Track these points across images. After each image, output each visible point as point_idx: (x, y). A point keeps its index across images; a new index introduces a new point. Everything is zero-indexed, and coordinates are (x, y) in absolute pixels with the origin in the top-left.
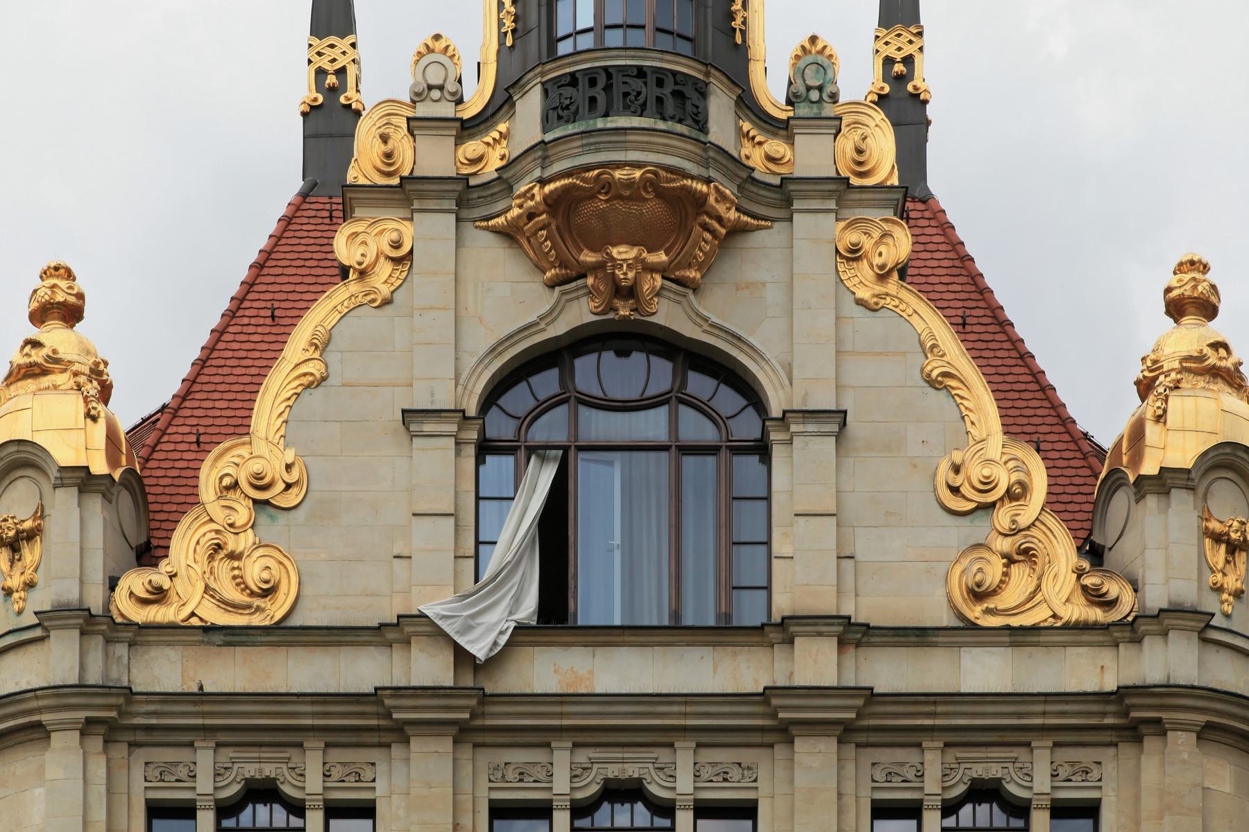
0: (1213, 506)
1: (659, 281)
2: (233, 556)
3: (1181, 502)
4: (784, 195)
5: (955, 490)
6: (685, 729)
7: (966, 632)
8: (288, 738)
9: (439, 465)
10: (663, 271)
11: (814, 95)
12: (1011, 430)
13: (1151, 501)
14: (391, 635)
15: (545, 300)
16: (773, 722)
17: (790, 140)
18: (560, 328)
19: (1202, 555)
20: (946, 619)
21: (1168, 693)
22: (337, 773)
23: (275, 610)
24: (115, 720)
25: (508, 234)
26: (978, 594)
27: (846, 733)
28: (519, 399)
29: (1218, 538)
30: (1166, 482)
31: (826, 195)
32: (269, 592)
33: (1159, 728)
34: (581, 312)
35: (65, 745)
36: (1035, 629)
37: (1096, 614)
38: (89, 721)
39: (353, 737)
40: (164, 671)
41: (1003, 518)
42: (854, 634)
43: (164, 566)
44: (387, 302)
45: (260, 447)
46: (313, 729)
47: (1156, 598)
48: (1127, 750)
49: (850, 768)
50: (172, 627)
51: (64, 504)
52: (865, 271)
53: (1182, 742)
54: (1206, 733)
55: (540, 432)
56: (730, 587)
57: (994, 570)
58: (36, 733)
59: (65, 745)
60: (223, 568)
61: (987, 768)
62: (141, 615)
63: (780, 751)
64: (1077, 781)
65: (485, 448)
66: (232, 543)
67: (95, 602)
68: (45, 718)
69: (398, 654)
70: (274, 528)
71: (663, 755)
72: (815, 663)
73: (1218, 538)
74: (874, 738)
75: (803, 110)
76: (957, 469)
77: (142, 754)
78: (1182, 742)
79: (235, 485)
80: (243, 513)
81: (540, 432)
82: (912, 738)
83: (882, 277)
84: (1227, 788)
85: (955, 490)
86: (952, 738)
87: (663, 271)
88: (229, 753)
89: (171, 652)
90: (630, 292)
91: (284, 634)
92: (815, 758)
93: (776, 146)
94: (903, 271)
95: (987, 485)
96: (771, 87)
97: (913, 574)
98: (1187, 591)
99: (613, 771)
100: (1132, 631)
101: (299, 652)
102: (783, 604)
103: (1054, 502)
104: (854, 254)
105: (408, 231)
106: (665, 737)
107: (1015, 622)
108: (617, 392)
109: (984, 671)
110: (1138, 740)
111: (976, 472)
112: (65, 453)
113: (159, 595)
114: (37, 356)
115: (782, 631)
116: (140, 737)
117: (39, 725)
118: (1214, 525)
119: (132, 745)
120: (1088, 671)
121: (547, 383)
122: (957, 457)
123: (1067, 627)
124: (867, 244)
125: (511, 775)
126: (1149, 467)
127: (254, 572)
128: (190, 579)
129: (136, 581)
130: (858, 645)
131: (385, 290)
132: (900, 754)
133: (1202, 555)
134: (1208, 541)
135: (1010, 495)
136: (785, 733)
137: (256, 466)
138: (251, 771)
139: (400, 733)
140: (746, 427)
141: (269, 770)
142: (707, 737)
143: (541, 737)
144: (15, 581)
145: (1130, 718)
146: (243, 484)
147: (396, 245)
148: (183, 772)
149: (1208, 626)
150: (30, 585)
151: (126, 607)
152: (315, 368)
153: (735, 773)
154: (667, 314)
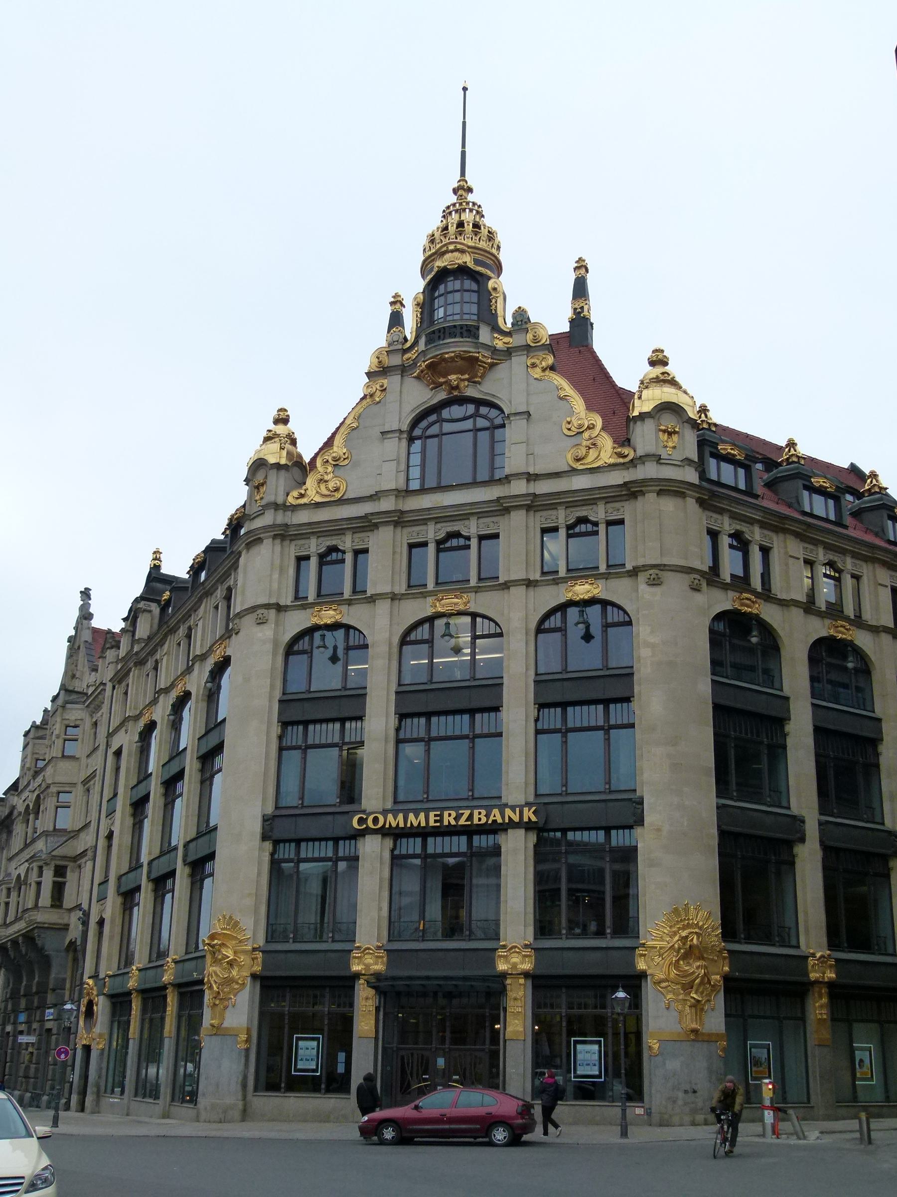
0: (662, 421)
1: (466, 383)
2: (326, 481)
3: (649, 425)
4: (509, 352)
5: (569, 429)
6: (473, 514)
7: (573, 471)
8: (341, 532)
9: (395, 447)
10: (468, 380)
11: (520, 323)
12: (590, 408)
13: (639, 423)
14: (375, 498)
15: (431, 394)
16: (502, 508)
17: (511, 337)
18: (435, 401)
19: (657, 438)
20: (566, 468)
21: (645, 482)
22: (356, 541)
23: (338, 495)
24: (283, 534)
25: (418, 378)
26: (578, 460)
27: (529, 508)
28: (424, 424)
29: (664, 431)
30: (642, 416)
31: (523, 350)
32: (337, 490)
33: (643, 493)
34: (442, 395)
35: (268, 542)
36: (598, 467)
37: (621, 460)
38: (275, 535)
39: (362, 529)
40: (303, 517)
41: (586, 435)
42: (531, 477)
43: (304, 487)
44: (378, 403)
45: (335, 449)
46: (348, 528)
47: (640, 452)
48: (632, 502)
49: (531, 519)
50: (305, 504)
51: (273, 474)
52: (538, 370)
53: (651, 497)
54: (660, 493)
55: (430, 432)
56: (492, 469)
57: (582, 451)
58: (259, 540)
59: (268, 542)
60: (323, 486)
61: (582, 512)
62: (294, 502)
63: (506, 516)
64: (615, 513)
65: (411, 440)
66: (326, 478)
67: (280, 501)
68: (261, 536)
69: (377, 503)
70: (340, 472)
71: (466, 522)
72: (519, 487)
73: (664, 431)
74: (541, 508)
75: (516, 328)
76: (569, 423)
77: (294, 543)
78: (651, 497)
79: (328, 461)
80: (330, 469)
81: (430, 432)
82: (553, 507)
83: (544, 370)
84: (671, 509)
85: (569, 429)
86: (568, 505)
87: (468, 380)
88: (322, 539)
89: (305, 511)
90: (457, 387)
91: (341, 502)
92: (518, 517)
93: (506, 340)
94: (552, 368)
95: (580, 426)
96: (507, 321)
97: (554, 455)
98: (651, 449)
99: (449, 529)
100: (633, 463)
101: (346, 507)
102: (507, 471)
103: (603, 429)
104: (534, 365)
105: (385, 382)
106: (466, 517)
107: (589, 467)
108: (455, 417)
109: (580, 483)
110: (636, 498)
111: (576, 423)
112: (272, 460)
113: (302, 496)
114: (270, 434)
115: (507, 479)
116: (293, 537)
117: (260, 538)
118: (663, 428)
119: (291, 540)
120: (617, 478)
121: (433, 417)
122: (569, 419)
123: (610, 465)
124: (538, 362)
125: (415, 534)
126: (636, 413)
127: (331, 485)
128: (312, 490)
129: (295, 493)
130: (535, 480)
131: (378, 399)
132: (550, 512)
133: (657, 438)
134: (661, 433)
135: (589, 428)
136: (507, 510)
137: (334, 455)
138: (329, 543)
139: (376, 526)
140: (498, 421)
141: (334, 543)
142: (480, 515)
143: (425, 522)
144: (258, 498)
145: (631, 491)
146: (330, 460)
147: (382, 386)
148: (307, 546)
149: (660, 459)
150: (262, 499)
151: (291, 500)
152: (354, 425)
153: (492, 525)
154: (471, 392)
